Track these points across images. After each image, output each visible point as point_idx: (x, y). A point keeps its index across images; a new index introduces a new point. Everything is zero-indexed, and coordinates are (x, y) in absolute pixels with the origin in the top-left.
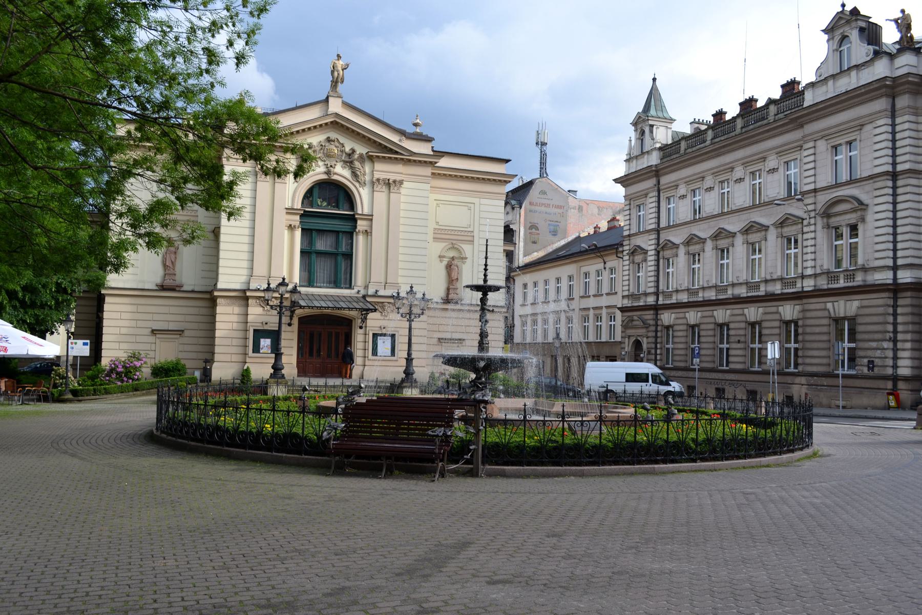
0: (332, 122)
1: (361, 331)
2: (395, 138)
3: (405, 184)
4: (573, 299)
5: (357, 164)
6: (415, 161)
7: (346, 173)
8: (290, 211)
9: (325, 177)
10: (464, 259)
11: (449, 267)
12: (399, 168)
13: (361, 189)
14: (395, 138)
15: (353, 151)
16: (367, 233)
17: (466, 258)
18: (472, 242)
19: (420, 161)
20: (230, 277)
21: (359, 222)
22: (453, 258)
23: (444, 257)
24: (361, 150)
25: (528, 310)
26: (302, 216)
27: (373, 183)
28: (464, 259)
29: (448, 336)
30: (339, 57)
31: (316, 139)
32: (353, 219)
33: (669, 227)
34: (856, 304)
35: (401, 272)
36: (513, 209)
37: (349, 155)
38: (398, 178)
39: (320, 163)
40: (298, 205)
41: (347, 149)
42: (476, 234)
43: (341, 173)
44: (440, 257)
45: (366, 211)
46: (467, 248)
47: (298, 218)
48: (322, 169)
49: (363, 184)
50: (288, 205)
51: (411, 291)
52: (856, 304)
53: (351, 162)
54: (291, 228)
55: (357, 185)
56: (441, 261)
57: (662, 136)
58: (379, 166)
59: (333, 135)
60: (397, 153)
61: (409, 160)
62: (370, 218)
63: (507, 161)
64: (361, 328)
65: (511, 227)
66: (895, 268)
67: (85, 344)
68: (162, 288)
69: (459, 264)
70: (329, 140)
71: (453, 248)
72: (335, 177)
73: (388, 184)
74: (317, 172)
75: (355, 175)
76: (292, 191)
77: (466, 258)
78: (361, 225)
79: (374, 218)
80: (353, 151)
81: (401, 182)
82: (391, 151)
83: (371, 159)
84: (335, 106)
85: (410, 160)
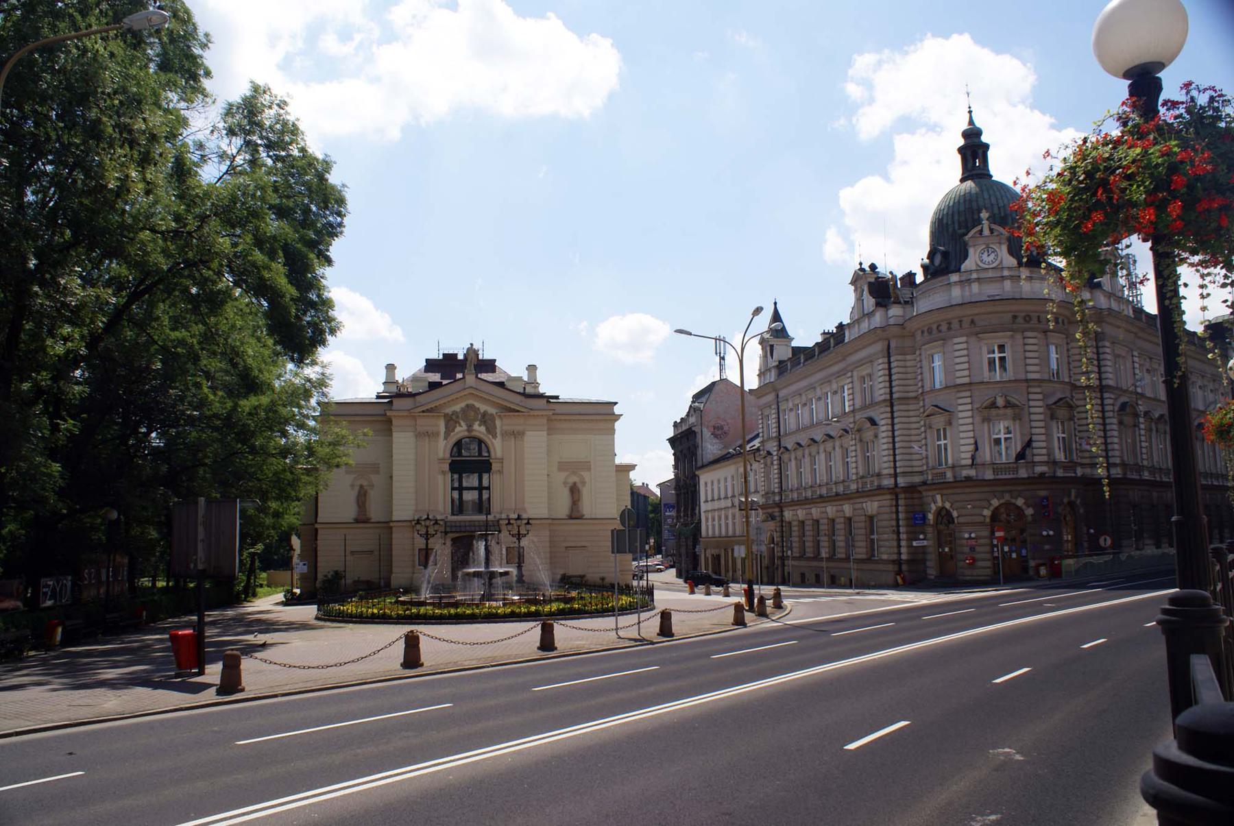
3: (528, 433)
7: (483, 429)
8: (441, 460)
16: (500, 472)
18: (589, 469)
20: (404, 509)
25: (710, 506)
27: (502, 435)
28: (584, 483)
33: (786, 435)
34: (876, 504)
38: (520, 428)
40: (448, 455)
43: (479, 430)
45: (499, 454)
46: (585, 474)
48: (465, 427)
49: (495, 436)
50: (441, 455)
52: (876, 504)
54: (443, 473)
57: (783, 353)
62: (501, 461)
66: (895, 475)
68: (357, 521)
72: (474, 434)
74: (460, 431)
75: (487, 429)
76: (443, 448)
78: (495, 467)
81: (523, 434)
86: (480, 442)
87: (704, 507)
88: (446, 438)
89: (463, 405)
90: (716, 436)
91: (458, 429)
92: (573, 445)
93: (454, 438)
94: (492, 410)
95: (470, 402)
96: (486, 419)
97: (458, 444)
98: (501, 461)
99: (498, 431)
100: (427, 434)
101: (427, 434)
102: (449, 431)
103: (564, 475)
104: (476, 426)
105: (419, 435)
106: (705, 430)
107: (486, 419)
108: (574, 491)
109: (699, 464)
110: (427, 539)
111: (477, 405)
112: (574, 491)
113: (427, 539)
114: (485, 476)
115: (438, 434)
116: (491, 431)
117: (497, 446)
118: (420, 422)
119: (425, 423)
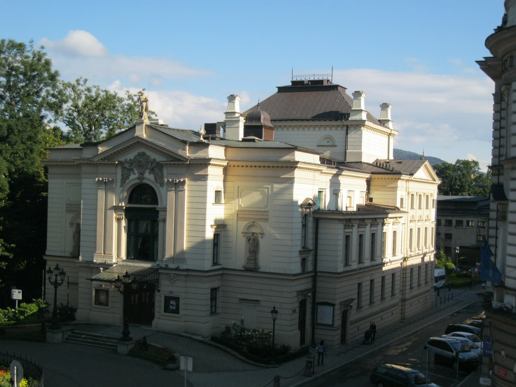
5: (156, 170)
7: (152, 177)
9: (138, 181)
13: (161, 188)
16: (164, 221)
21: (160, 213)
28: (262, 234)
31: (131, 156)
32: (156, 212)
39: (136, 171)
43: (149, 178)
44: (243, 233)
48: (137, 175)
49: (162, 185)
56: (244, 237)
59: (142, 150)
67: (19, 292)
72: (145, 181)
74: (134, 178)
75: (156, 179)
88: (122, 186)
91: (132, 177)
94: (159, 158)
102: (125, 178)
110: (56, 287)
111: (148, 153)
113: (56, 287)
116: (159, 179)
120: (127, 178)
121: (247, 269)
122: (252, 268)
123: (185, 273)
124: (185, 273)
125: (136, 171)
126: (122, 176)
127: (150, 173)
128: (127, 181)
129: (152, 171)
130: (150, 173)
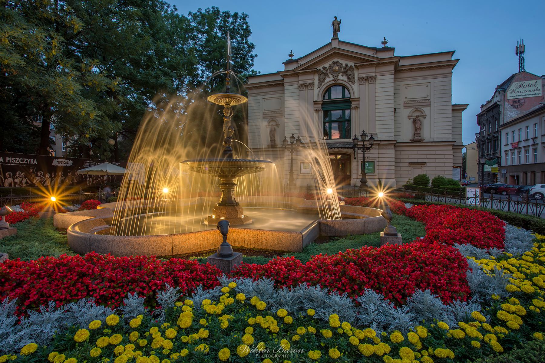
0: (334, 53)
1: (355, 160)
2: (370, 53)
3: (378, 78)
4: (537, 137)
5: (349, 72)
6: (382, 63)
7: (345, 78)
8: (316, 103)
9: (333, 82)
10: (424, 116)
11: (415, 122)
12: (373, 69)
14: (370, 53)
15: (347, 65)
17: (426, 115)
19: (386, 63)
21: (353, 103)
22: (417, 116)
23: (412, 116)
24: (351, 64)
26: (322, 105)
27: (359, 80)
28: (424, 116)
29: (415, 161)
30: (336, 18)
31: (327, 65)
35: (378, 127)
36: (499, 93)
37: (345, 68)
38: (373, 74)
39: (330, 76)
40: (320, 99)
41: (344, 65)
42: (432, 100)
43: (342, 78)
44: (408, 117)
45: (356, 96)
46: (426, 110)
47: (320, 106)
48: (332, 78)
49: (353, 82)
50: (315, 99)
51: (363, 135)
53: (346, 72)
54: (317, 111)
55: (350, 83)
56: (410, 119)
58: (361, 71)
59: (335, 60)
60: (371, 61)
61: (379, 64)
63: (453, 52)
64: (355, 158)
65: (498, 103)
69: (421, 119)
70: (334, 63)
71: (417, 110)
72: (338, 82)
73: (367, 79)
74: (329, 80)
76: (316, 93)
77: (426, 115)
78: (354, 104)
79: (360, 99)
80: (347, 65)
82: (367, 61)
83: (357, 67)
84: (335, 44)
85: (380, 63)
86: (344, 87)
87: (504, 148)
89: (331, 63)
90: (514, 106)
91: (327, 80)
92: (415, 89)
93: (324, 86)
94: (351, 64)
95: (335, 60)
96: (347, 71)
97: (328, 90)
98: (358, 100)
99: (356, 78)
100: (306, 85)
101: (306, 85)
102: (321, 81)
103: (408, 111)
104: (340, 77)
105: (301, 86)
106: (506, 104)
107: (347, 71)
108: (417, 123)
109: (502, 123)
111: (341, 61)
112: (417, 123)
114: (347, 112)
115: (312, 84)
116: (351, 79)
117: (356, 89)
118: (301, 78)
119: (304, 79)
120: (324, 81)
121: (414, 141)
122: (417, 140)
123: (379, 142)
124: (379, 142)
125: (330, 76)
126: (319, 80)
127: (342, 76)
128: (323, 84)
129: (345, 73)
130: (342, 76)
